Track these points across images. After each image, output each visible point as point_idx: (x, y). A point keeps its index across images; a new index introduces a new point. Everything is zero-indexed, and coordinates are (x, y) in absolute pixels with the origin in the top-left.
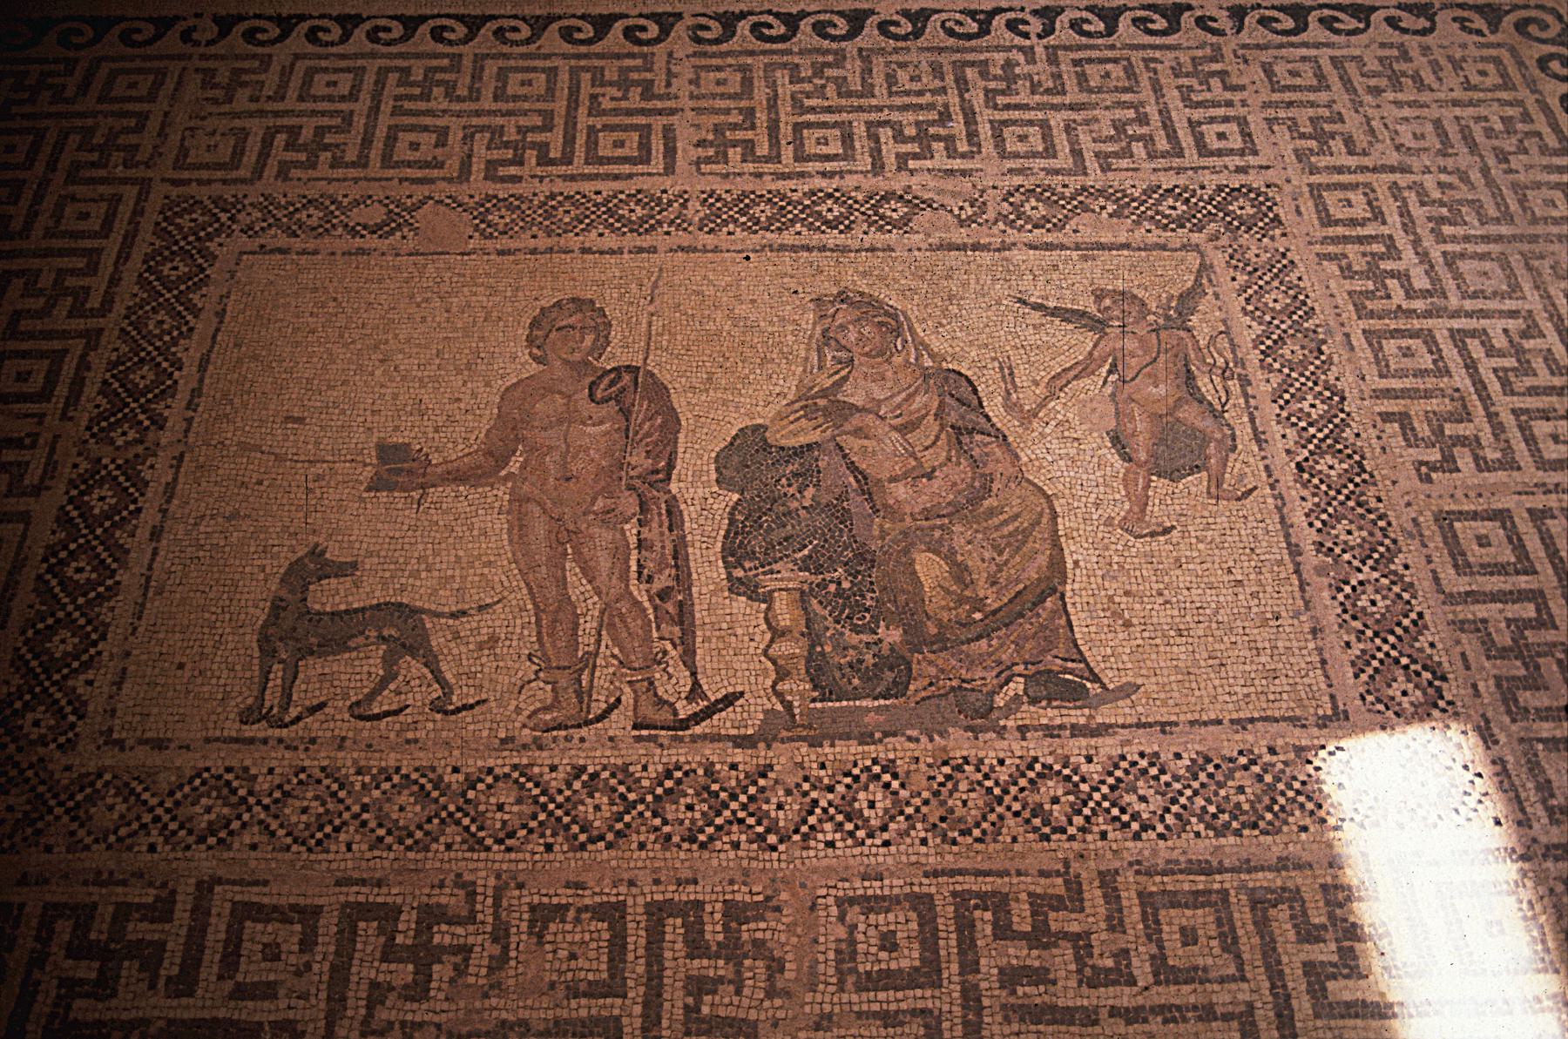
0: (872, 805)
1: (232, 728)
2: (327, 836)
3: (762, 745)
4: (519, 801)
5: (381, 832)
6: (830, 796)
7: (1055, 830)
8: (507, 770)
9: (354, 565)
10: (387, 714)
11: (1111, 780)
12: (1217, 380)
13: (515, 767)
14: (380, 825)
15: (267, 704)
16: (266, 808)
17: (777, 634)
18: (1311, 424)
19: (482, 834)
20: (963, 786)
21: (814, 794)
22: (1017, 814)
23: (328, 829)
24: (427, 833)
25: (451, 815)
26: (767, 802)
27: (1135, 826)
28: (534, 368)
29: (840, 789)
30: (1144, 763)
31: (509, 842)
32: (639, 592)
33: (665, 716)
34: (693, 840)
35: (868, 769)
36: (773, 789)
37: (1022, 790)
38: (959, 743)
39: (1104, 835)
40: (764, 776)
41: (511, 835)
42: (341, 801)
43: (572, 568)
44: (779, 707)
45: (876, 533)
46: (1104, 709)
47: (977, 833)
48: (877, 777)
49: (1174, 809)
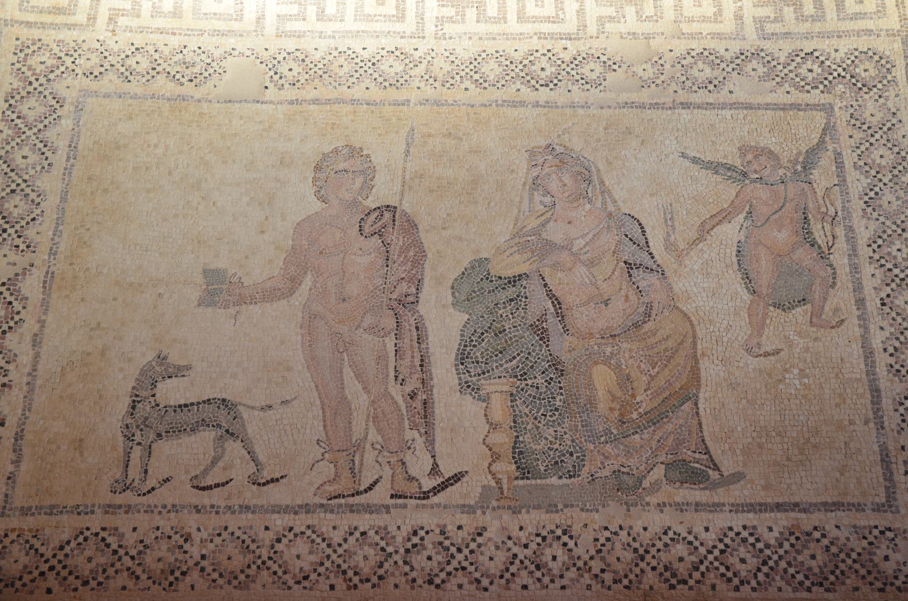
0: (554, 558)
1: (105, 497)
2: (177, 579)
3: (479, 512)
4: (310, 553)
5: (215, 575)
6: (525, 550)
7: (679, 582)
8: (303, 529)
9: (188, 368)
10: (217, 485)
11: (721, 546)
12: (828, 227)
13: (309, 527)
14: (214, 570)
15: (130, 477)
16: (133, 558)
17: (494, 427)
18: (896, 266)
19: (287, 577)
20: (618, 546)
21: (515, 550)
22: (654, 569)
23: (177, 574)
24: (248, 576)
25: (264, 563)
26: (482, 554)
27: (736, 581)
28: (318, 206)
29: (533, 546)
30: (745, 534)
31: (306, 583)
32: (396, 391)
33: (413, 489)
34: (430, 582)
35: (553, 532)
36: (486, 545)
37: (659, 550)
38: (613, 514)
39: (713, 587)
40: (480, 535)
41: (306, 578)
42: (186, 552)
43: (348, 373)
44: (493, 483)
45: (562, 346)
46: (720, 491)
47: (626, 582)
48: (559, 538)
49: (765, 569)
